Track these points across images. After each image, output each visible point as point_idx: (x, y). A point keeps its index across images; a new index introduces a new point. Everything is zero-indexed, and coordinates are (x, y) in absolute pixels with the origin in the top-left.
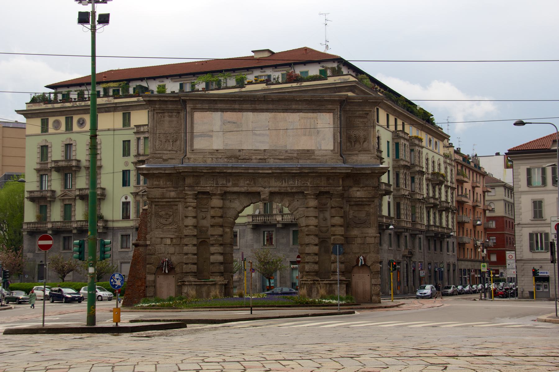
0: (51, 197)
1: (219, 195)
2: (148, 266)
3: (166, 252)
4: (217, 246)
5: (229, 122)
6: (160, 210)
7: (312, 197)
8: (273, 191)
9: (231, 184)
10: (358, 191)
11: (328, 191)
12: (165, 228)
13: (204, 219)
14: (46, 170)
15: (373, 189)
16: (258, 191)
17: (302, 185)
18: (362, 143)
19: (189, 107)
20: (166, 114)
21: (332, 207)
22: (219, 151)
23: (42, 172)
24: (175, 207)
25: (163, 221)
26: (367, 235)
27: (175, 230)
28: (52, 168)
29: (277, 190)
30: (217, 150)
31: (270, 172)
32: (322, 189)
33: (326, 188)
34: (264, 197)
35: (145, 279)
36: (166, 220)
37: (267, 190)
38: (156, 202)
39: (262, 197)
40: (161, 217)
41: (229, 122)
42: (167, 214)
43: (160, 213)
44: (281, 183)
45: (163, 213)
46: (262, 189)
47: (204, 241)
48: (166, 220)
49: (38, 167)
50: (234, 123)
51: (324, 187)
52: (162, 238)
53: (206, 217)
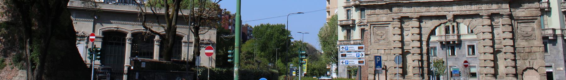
0: (352, 24)
1: (417, 18)
2: (369, 69)
4: (416, 55)
6: (377, 30)
7: (486, 17)
8: (455, 14)
9: (424, 10)
10: (523, 11)
11: (498, 12)
12: (380, 42)
13: (407, 36)
14: (349, 7)
15: (536, 9)
16: (445, 14)
17: (477, 9)
21: (503, 25)
23: (348, 9)
25: (379, 37)
26: (533, 45)
27: (387, 44)
28: (353, 5)
29: (458, 13)
32: (494, 12)
33: (496, 11)
34: (449, 19)
35: (368, 78)
36: (381, 37)
37: (452, 13)
38: (373, 24)
39: (448, 19)
40: (377, 35)
43: (377, 33)
44: (461, 8)
45: (379, 32)
47: (408, 51)
48: (381, 37)
49: (345, 5)
51: (495, 9)
52: (378, 50)
53: (408, 35)
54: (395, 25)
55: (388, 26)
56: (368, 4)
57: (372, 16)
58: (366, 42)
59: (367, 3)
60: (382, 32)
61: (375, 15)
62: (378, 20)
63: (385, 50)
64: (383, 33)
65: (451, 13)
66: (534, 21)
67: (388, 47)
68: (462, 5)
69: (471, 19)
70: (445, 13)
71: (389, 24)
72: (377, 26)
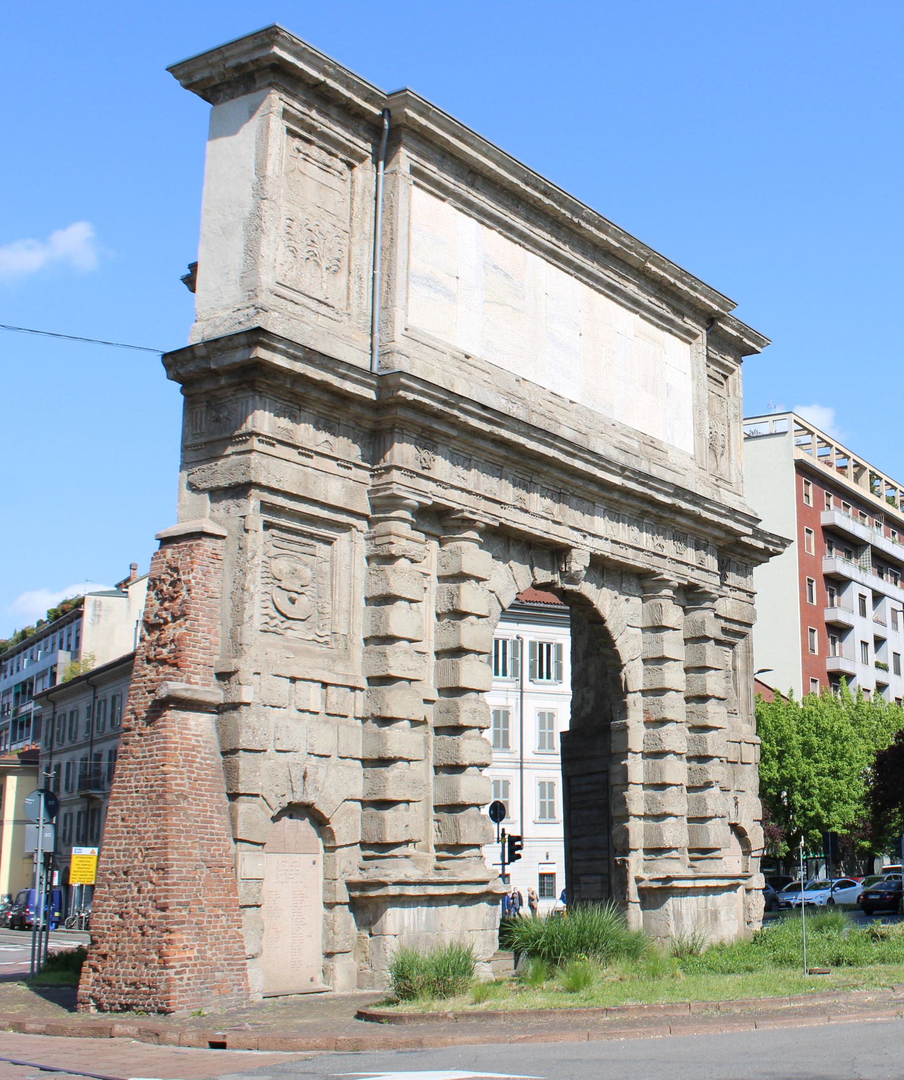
3: (304, 749)
5: (495, 267)
6: (274, 551)
16: (570, 543)
18: (718, 457)
19: (405, 158)
20: (314, 151)
22: (470, 361)
24: (321, 549)
29: (605, 549)
30: (467, 357)
31: (617, 480)
41: (495, 267)
42: (294, 572)
46: (577, 536)
50: (507, 276)
52: (293, 680)
54: (404, 542)
55: (329, 542)
56: (299, 367)
57: (280, 450)
58: (203, 620)
59: (295, 358)
60: (294, 572)
61: (292, 454)
62: (306, 487)
63: (325, 685)
64: (300, 578)
65: (589, 540)
66: (736, 640)
67: (339, 668)
68: (618, 522)
69: (616, 593)
70: (561, 534)
71: (346, 528)
72: (283, 522)
